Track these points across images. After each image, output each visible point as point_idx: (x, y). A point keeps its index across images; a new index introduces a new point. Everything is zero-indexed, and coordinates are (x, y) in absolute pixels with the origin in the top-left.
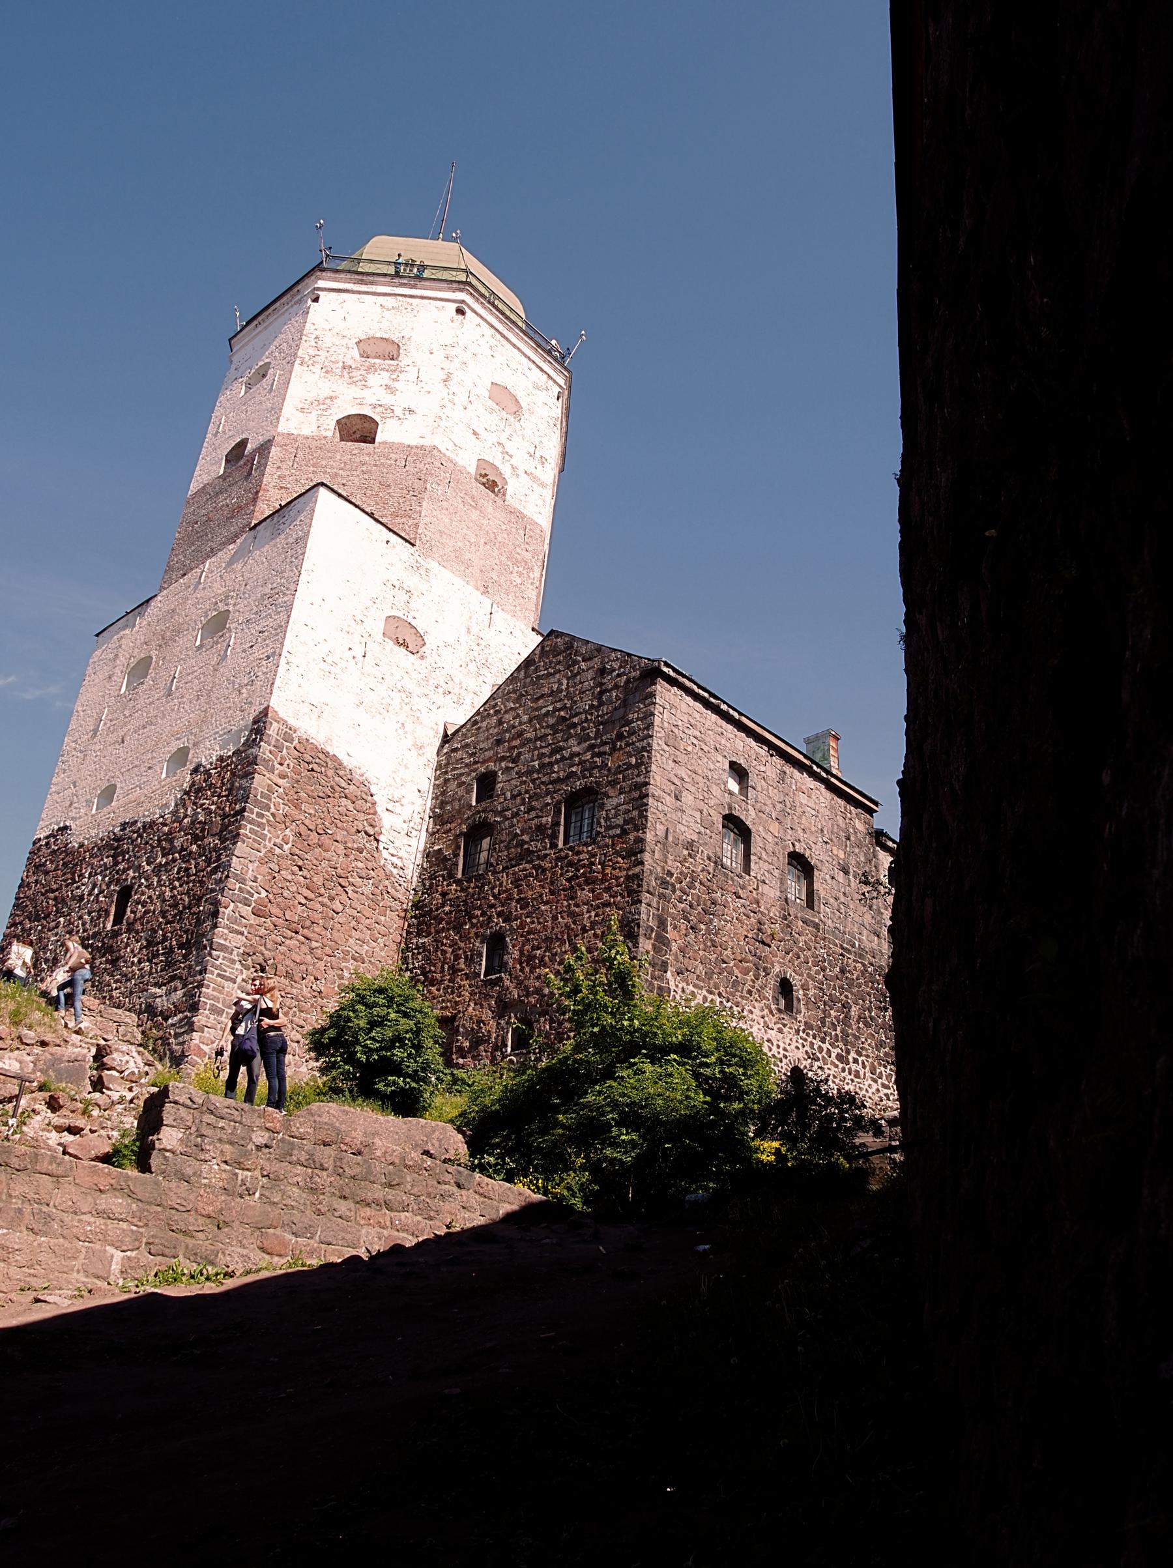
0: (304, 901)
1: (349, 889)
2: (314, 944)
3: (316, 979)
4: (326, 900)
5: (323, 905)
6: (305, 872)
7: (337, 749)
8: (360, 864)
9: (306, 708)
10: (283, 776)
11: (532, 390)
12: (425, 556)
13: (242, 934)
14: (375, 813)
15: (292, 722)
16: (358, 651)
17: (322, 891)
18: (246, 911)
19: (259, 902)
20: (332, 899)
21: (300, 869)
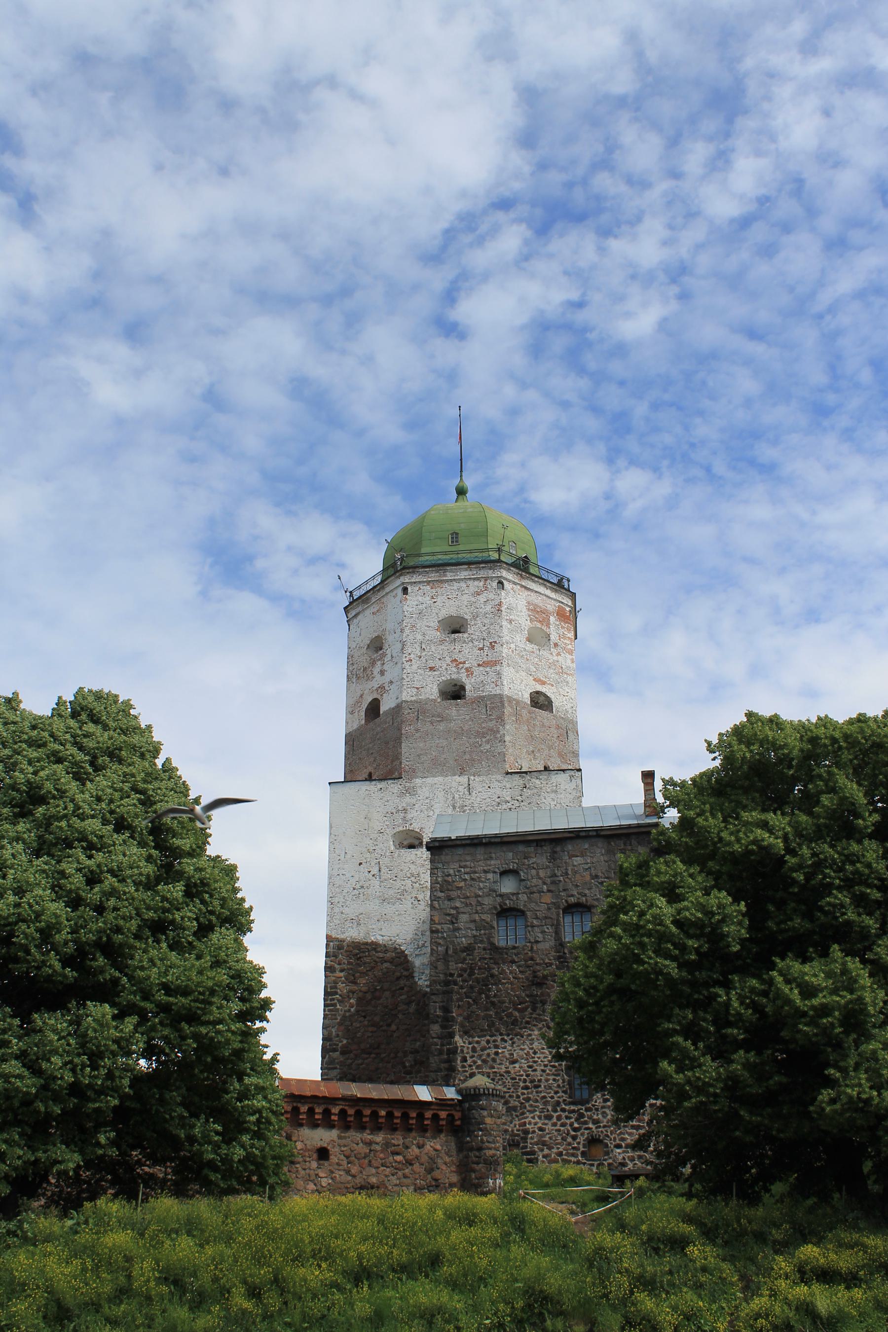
0: (370, 1034)
1: (400, 1016)
2: (383, 1055)
3: (388, 1075)
4: (384, 1028)
5: (384, 1031)
6: (368, 1018)
7: (376, 937)
8: (403, 997)
9: (348, 924)
10: (342, 971)
11: (473, 599)
12: (410, 779)
13: (336, 1068)
14: (408, 961)
15: (342, 937)
16: (375, 870)
17: (381, 1023)
18: (336, 1055)
19: (344, 1046)
20: (389, 1025)
21: (365, 1017)
